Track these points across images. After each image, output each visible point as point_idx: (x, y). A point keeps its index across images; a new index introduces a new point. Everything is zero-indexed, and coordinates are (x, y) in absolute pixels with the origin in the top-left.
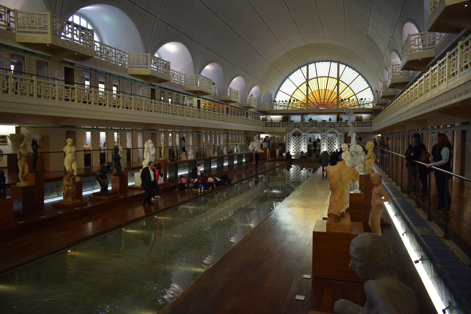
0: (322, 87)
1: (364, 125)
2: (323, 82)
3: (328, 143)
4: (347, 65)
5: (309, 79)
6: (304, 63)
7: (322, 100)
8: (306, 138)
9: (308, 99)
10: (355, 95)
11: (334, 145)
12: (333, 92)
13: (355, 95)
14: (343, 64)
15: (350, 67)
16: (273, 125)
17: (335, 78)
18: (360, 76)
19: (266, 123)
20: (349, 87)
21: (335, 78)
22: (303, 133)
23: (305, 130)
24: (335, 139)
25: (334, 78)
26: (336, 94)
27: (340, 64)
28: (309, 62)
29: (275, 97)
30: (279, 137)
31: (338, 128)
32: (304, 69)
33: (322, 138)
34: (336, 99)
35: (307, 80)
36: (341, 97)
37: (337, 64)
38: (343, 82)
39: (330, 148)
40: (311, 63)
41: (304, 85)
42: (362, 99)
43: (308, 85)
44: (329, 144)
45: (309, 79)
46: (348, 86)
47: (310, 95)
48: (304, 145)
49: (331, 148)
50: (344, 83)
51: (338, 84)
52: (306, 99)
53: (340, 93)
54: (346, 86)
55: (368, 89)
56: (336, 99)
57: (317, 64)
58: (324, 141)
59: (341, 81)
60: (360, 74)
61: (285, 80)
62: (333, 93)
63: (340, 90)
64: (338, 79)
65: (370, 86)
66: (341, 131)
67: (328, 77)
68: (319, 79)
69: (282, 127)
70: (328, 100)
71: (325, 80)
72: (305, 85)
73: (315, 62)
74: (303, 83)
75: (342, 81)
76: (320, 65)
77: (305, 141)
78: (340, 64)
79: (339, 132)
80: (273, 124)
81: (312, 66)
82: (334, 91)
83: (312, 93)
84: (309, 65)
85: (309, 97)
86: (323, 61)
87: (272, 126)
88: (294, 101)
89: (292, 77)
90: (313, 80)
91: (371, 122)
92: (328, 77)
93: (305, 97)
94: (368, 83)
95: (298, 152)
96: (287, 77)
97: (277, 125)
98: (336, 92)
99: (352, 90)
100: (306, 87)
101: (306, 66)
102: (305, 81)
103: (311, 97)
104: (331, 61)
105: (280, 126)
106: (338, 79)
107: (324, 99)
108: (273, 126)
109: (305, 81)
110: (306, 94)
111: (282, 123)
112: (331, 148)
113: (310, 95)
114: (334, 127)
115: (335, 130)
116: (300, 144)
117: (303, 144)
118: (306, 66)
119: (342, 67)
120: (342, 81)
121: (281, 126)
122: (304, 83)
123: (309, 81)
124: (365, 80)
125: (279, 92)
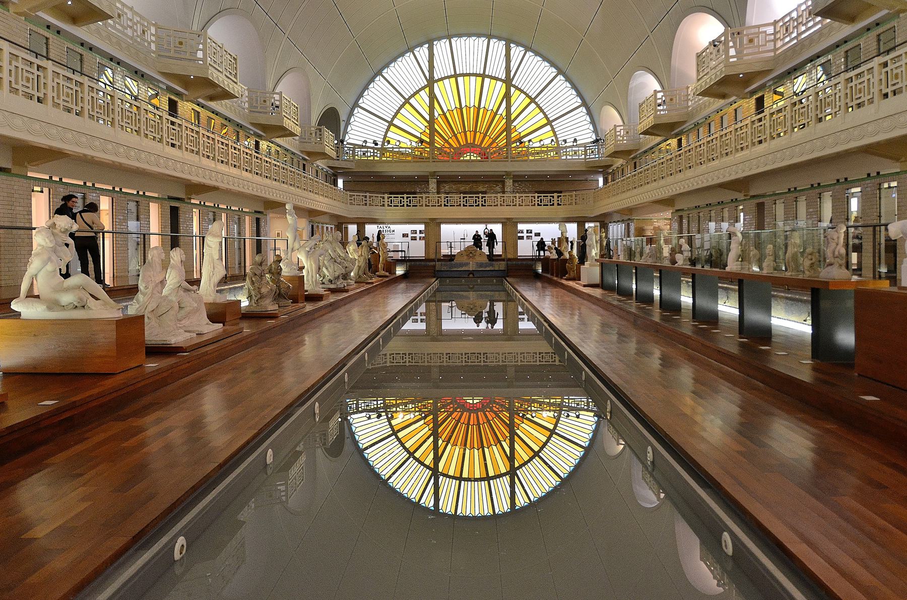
0: (470, 99)
2: (470, 86)
4: (528, 49)
7: (468, 133)
9: (433, 132)
12: (496, 114)
13: (549, 123)
14: (518, 44)
15: (537, 54)
17: (500, 80)
18: (561, 77)
21: (500, 80)
26: (504, 121)
28: (434, 35)
29: (348, 123)
32: (422, 53)
34: (505, 133)
35: (431, 82)
36: (517, 128)
37: (504, 43)
38: (520, 90)
40: (439, 39)
41: (422, 93)
43: (432, 97)
45: (436, 78)
46: (533, 100)
47: (439, 119)
50: (522, 91)
51: (507, 96)
52: (428, 131)
53: (513, 117)
54: (528, 100)
56: (505, 133)
59: (514, 86)
60: (560, 72)
61: (372, 80)
62: (498, 117)
63: (513, 109)
64: (508, 81)
65: (584, 104)
68: (460, 79)
71: (475, 82)
72: (424, 94)
73: (449, 37)
74: (420, 90)
75: (517, 88)
81: (441, 47)
83: (444, 114)
84: (435, 43)
85: (436, 127)
86: (469, 35)
90: (446, 81)
92: (483, 76)
93: (427, 125)
94: (579, 94)
96: (379, 73)
98: (504, 114)
99: (542, 110)
100: (427, 100)
102: (426, 83)
103: (441, 125)
104: (490, 37)
106: (508, 81)
109: (426, 83)
110: (427, 118)
113: (439, 119)
120: (517, 88)
122: (423, 88)
123: (435, 84)
124: (574, 87)
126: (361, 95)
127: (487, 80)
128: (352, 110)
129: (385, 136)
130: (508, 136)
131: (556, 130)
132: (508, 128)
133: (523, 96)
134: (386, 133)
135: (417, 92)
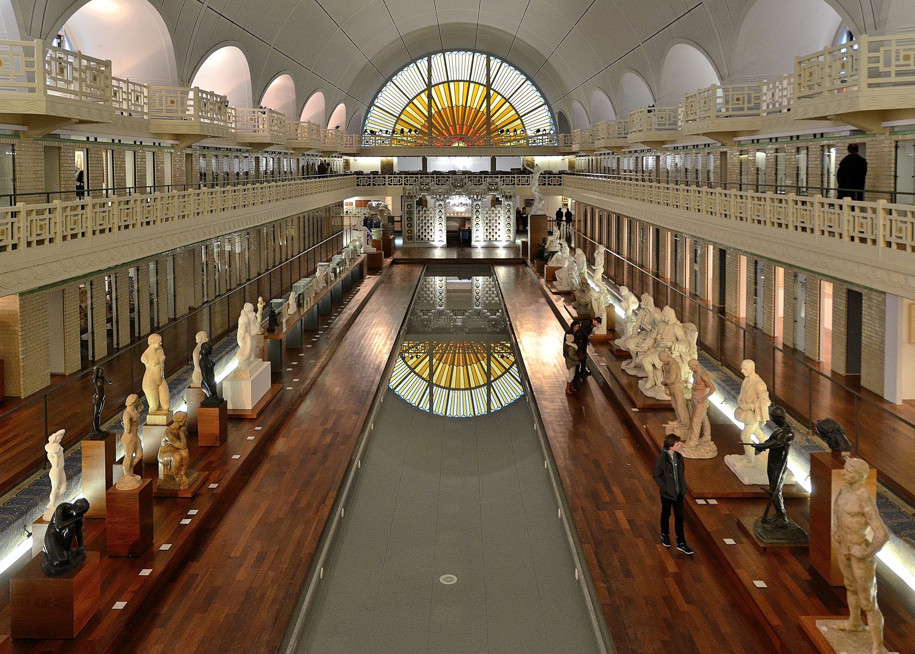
1: (547, 182)
3: (486, 222)
4: (504, 60)
5: (433, 84)
6: (422, 53)
8: (443, 210)
10: (520, 118)
11: (497, 225)
12: (479, 111)
14: (496, 57)
15: (510, 64)
17: (482, 85)
19: (358, 178)
20: (509, 103)
21: (482, 85)
24: (499, 213)
25: (480, 84)
27: (491, 58)
32: (423, 64)
33: (475, 210)
34: (485, 126)
35: (429, 86)
37: (485, 56)
38: (497, 92)
39: (489, 231)
40: (436, 53)
41: (423, 95)
42: (538, 131)
43: (430, 97)
44: (488, 222)
45: (433, 84)
46: (507, 100)
47: (436, 115)
49: (491, 231)
50: (499, 94)
51: (488, 97)
52: (427, 124)
53: (492, 114)
55: (543, 107)
56: (485, 126)
57: (447, 54)
58: (477, 217)
59: (493, 89)
60: (528, 78)
61: (384, 85)
62: (480, 113)
63: (492, 107)
64: (488, 86)
67: (470, 82)
69: (389, 184)
70: (470, 128)
76: (451, 57)
77: (440, 217)
78: (491, 58)
81: (437, 60)
82: (482, 110)
84: (433, 56)
85: (433, 120)
87: (369, 185)
88: (410, 131)
89: (399, 79)
90: (441, 86)
91: (560, 178)
95: (428, 239)
96: (390, 79)
98: (485, 112)
100: (426, 100)
101: (426, 58)
104: (474, 51)
105: (384, 184)
107: (462, 124)
108: (372, 184)
109: (426, 87)
110: (426, 114)
111: (389, 177)
112: (491, 231)
113: (436, 115)
114: (496, 190)
116: (431, 223)
118: (426, 58)
119: (496, 63)
120: (495, 91)
121: (387, 183)
123: (433, 88)
125: (374, 111)
126: (376, 97)
127: (472, 85)
128: (369, 108)
129: (394, 127)
130: (488, 129)
131: (524, 123)
132: (488, 121)
133: (500, 97)
134: (395, 126)
135: (419, 94)
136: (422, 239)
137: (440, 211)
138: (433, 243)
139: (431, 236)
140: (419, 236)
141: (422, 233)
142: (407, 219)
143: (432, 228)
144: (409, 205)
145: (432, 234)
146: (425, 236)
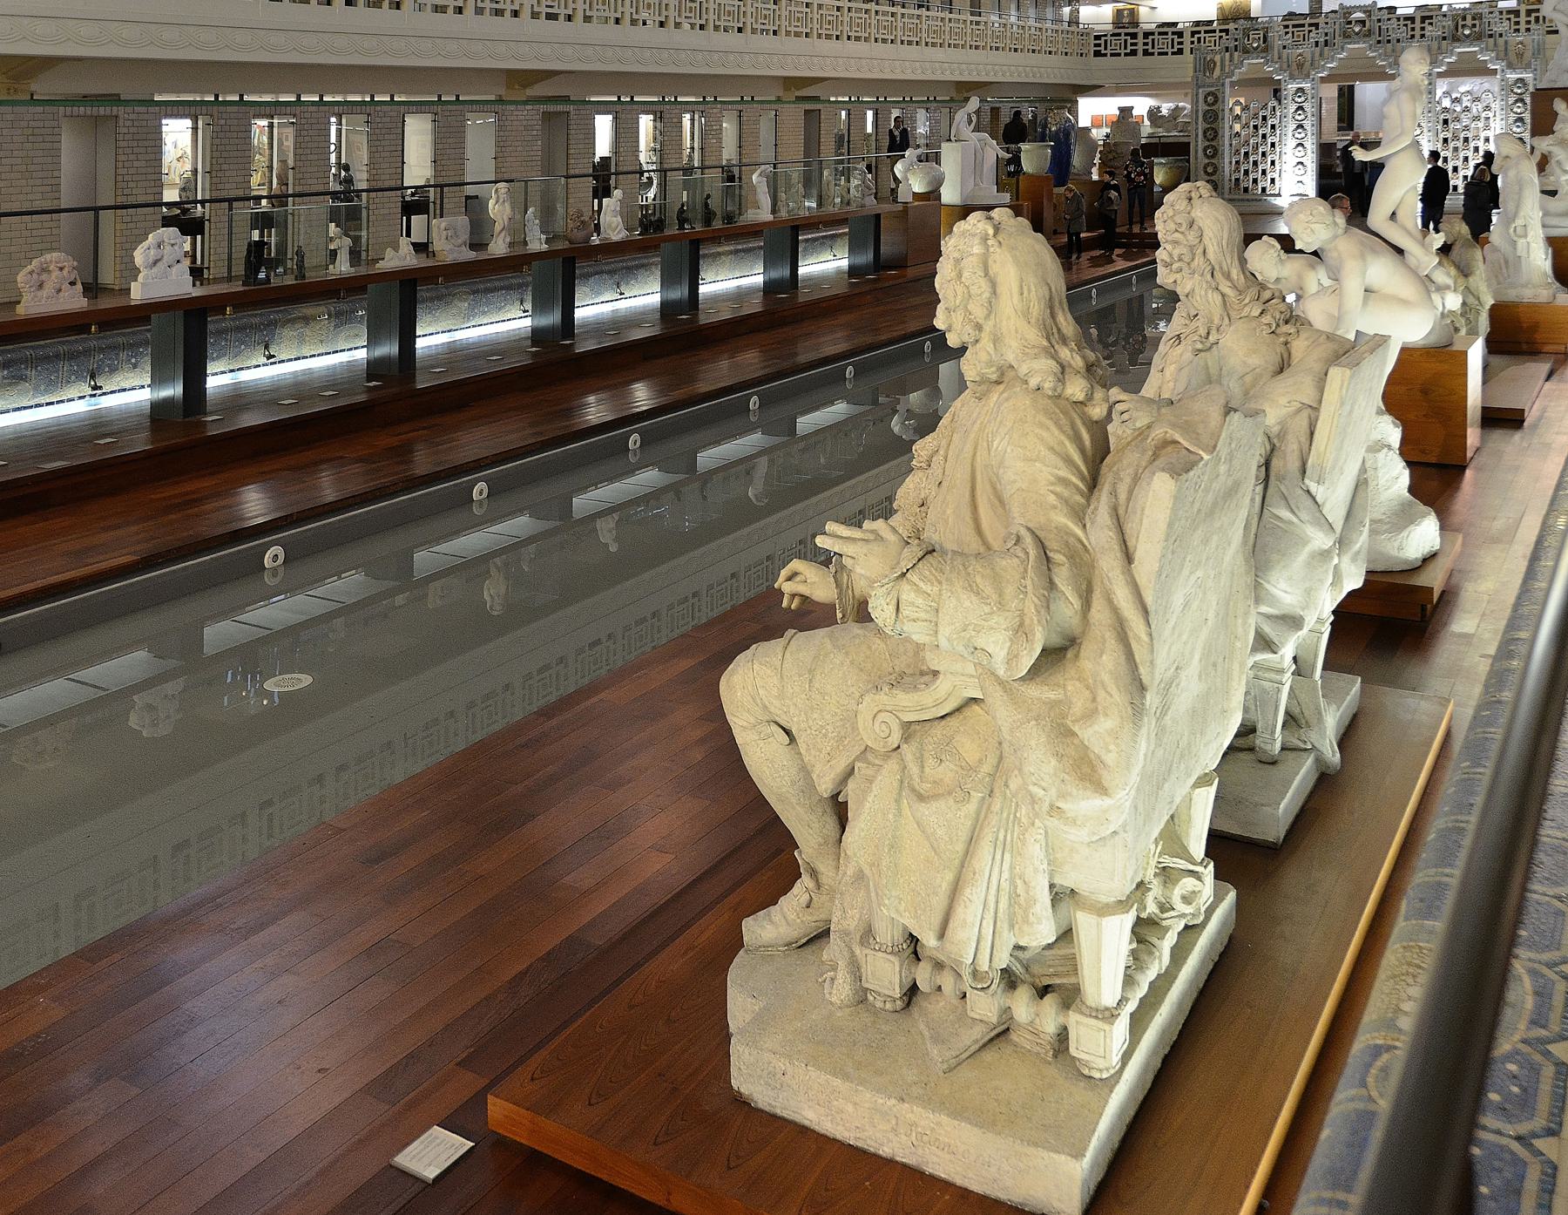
16: (1140, 48)
22: (1292, 77)
23: (1300, 66)
30: (1185, 108)
31: (1501, 41)
48: (1300, 152)
66: (1520, 55)
79: (1510, 66)
80: (1140, 39)
87: (1134, 53)
95: (1264, 189)
97: (1162, 43)
105: (1180, 52)
108: (1140, 52)
115: (1481, 51)
116: (1273, 145)
117: (1294, 143)
136: (1246, 190)
137: (1300, 108)
138: (1278, 201)
139: (1273, 181)
140: (1237, 180)
141: (1246, 172)
142: (1205, 133)
143: (1276, 158)
144: (1209, 94)
145: (1276, 175)
146: (1255, 181)
